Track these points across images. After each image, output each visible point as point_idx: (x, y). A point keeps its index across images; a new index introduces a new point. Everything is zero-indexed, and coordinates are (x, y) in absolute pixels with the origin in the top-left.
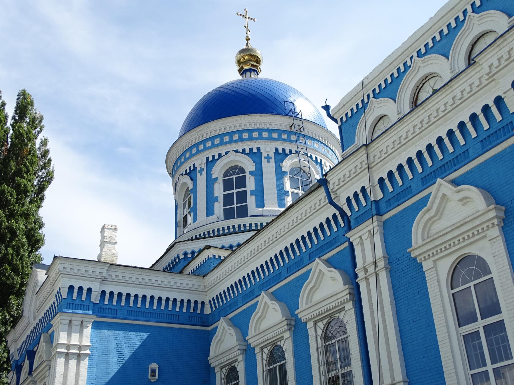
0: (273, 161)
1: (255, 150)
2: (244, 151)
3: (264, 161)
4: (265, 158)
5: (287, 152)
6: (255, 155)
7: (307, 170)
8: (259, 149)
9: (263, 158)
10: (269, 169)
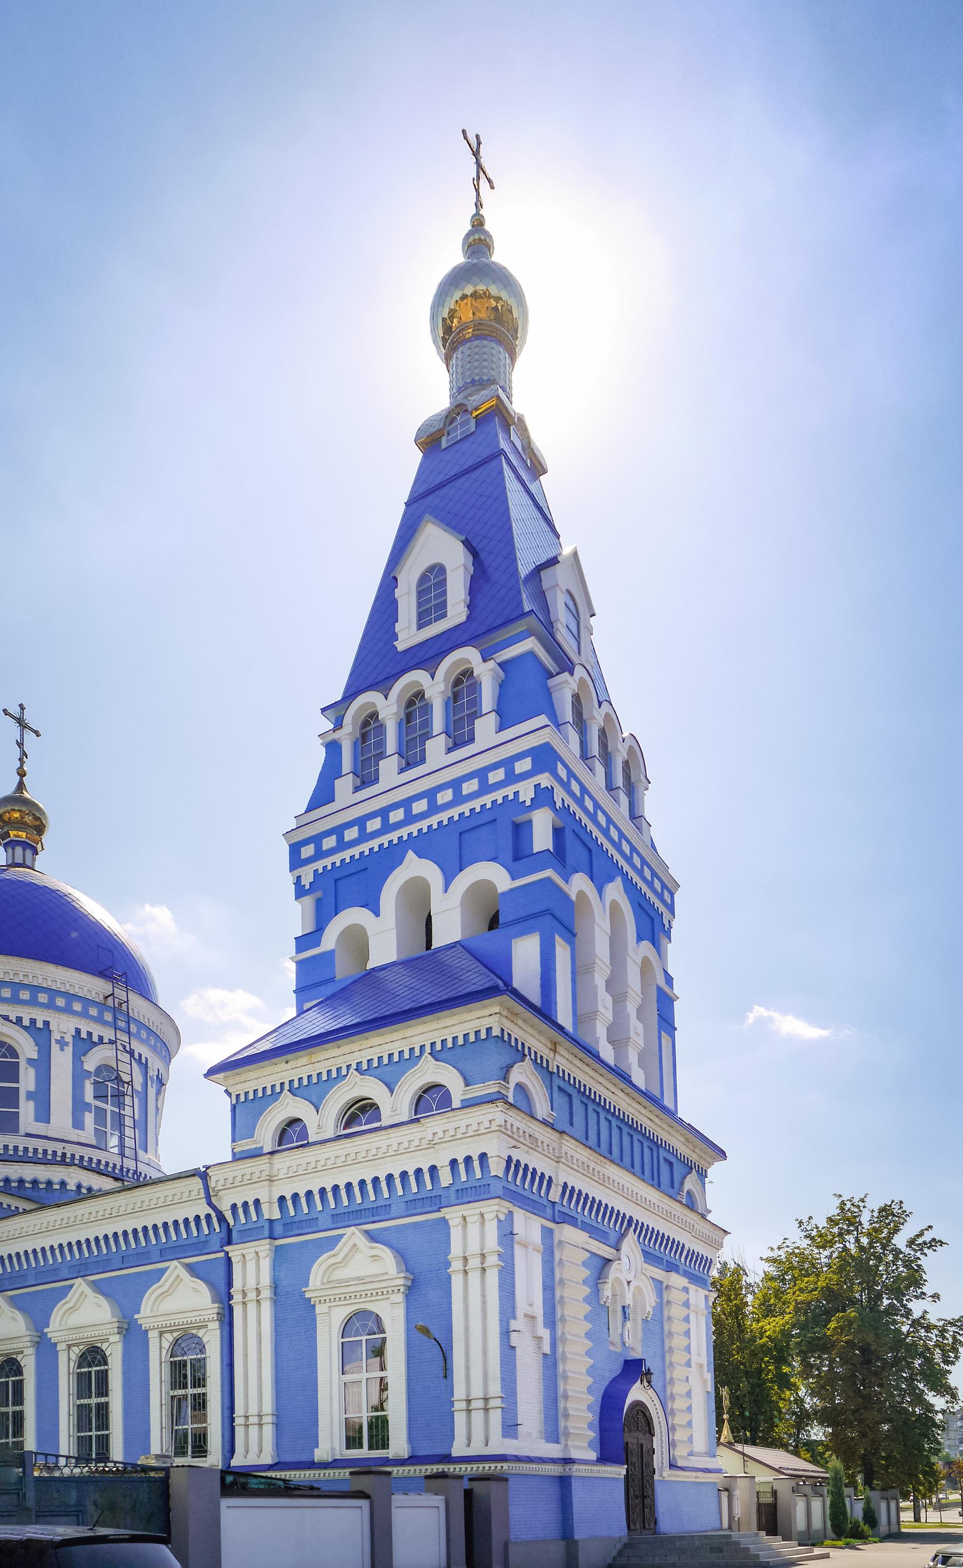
0: (69, 1049)
1: (40, 1025)
3: (55, 1047)
4: (57, 1041)
5: (95, 1039)
6: (40, 1033)
7: (126, 1078)
8: (47, 1024)
9: (53, 1041)
10: (61, 1061)
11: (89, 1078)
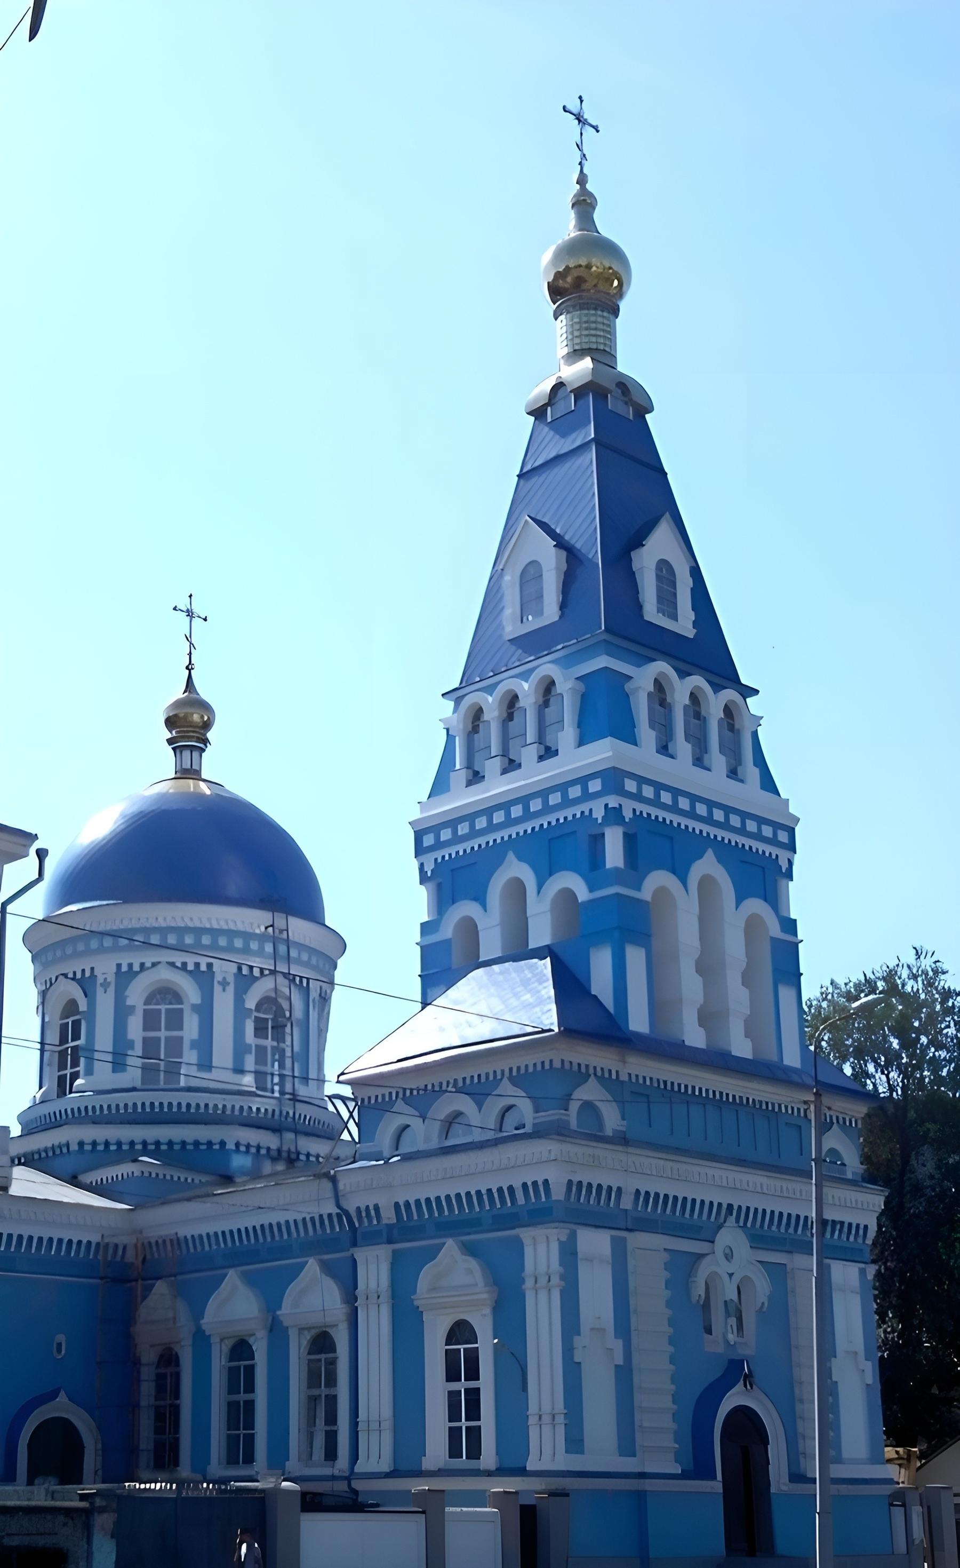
0: (231, 989)
1: (203, 968)
2: (184, 964)
3: (217, 989)
6: (204, 978)
8: (210, 966)
9: (216, 983)
10: (224, 1003)
11: (249, 1017)
